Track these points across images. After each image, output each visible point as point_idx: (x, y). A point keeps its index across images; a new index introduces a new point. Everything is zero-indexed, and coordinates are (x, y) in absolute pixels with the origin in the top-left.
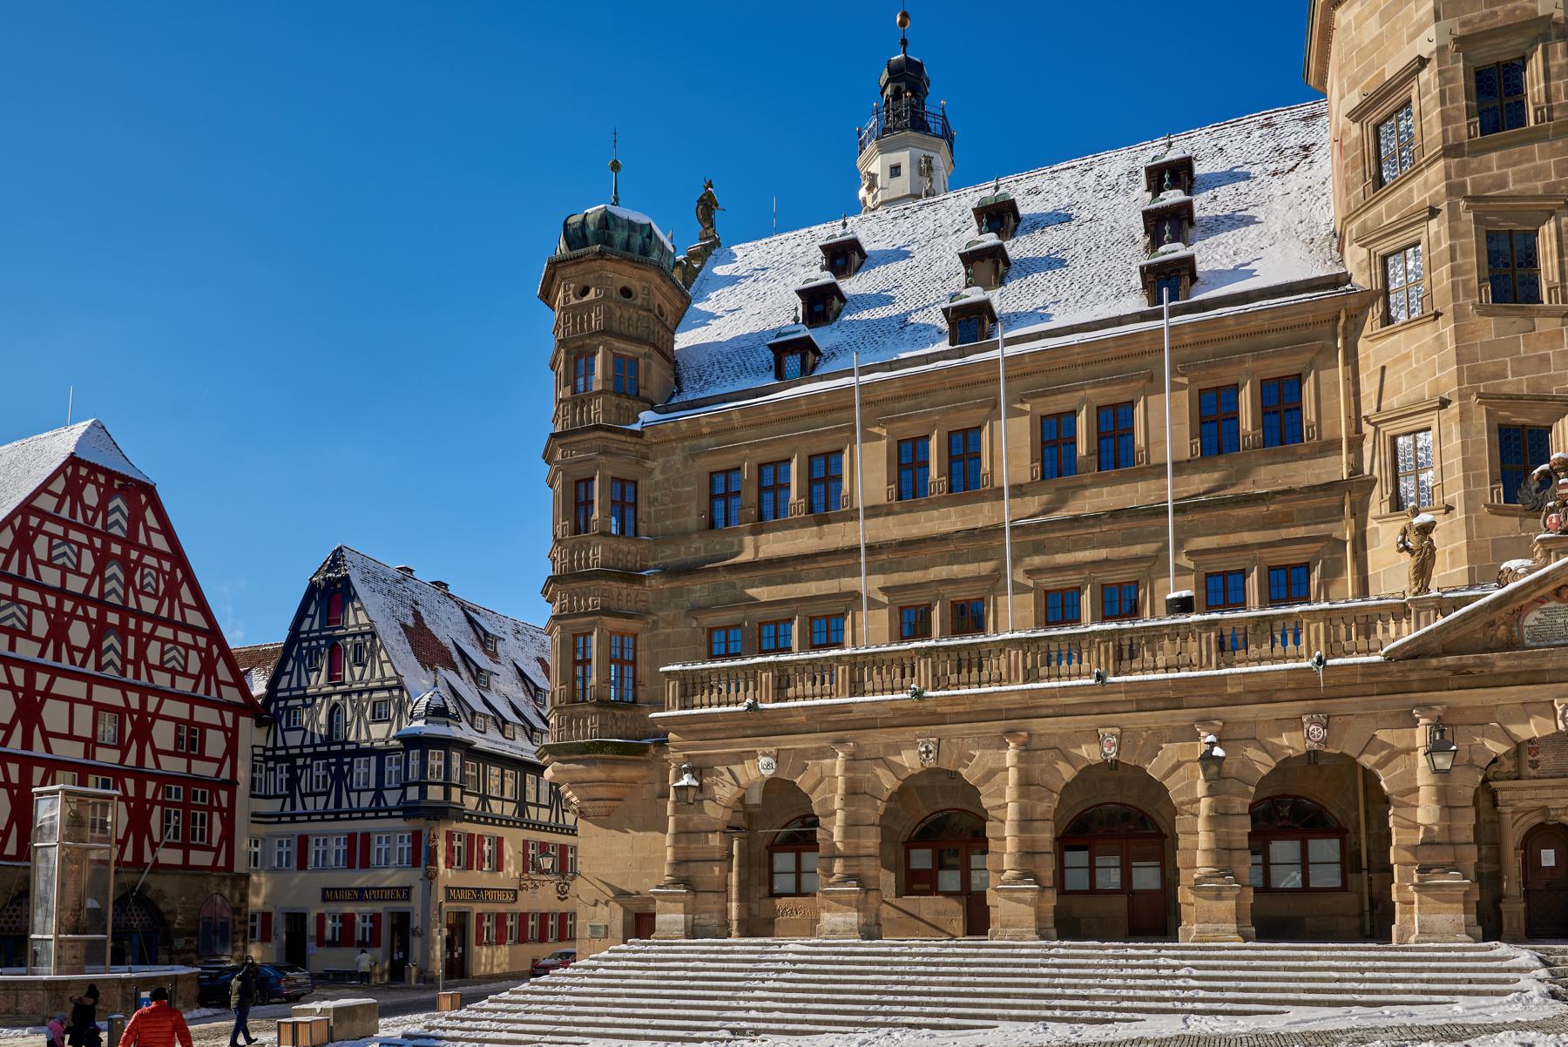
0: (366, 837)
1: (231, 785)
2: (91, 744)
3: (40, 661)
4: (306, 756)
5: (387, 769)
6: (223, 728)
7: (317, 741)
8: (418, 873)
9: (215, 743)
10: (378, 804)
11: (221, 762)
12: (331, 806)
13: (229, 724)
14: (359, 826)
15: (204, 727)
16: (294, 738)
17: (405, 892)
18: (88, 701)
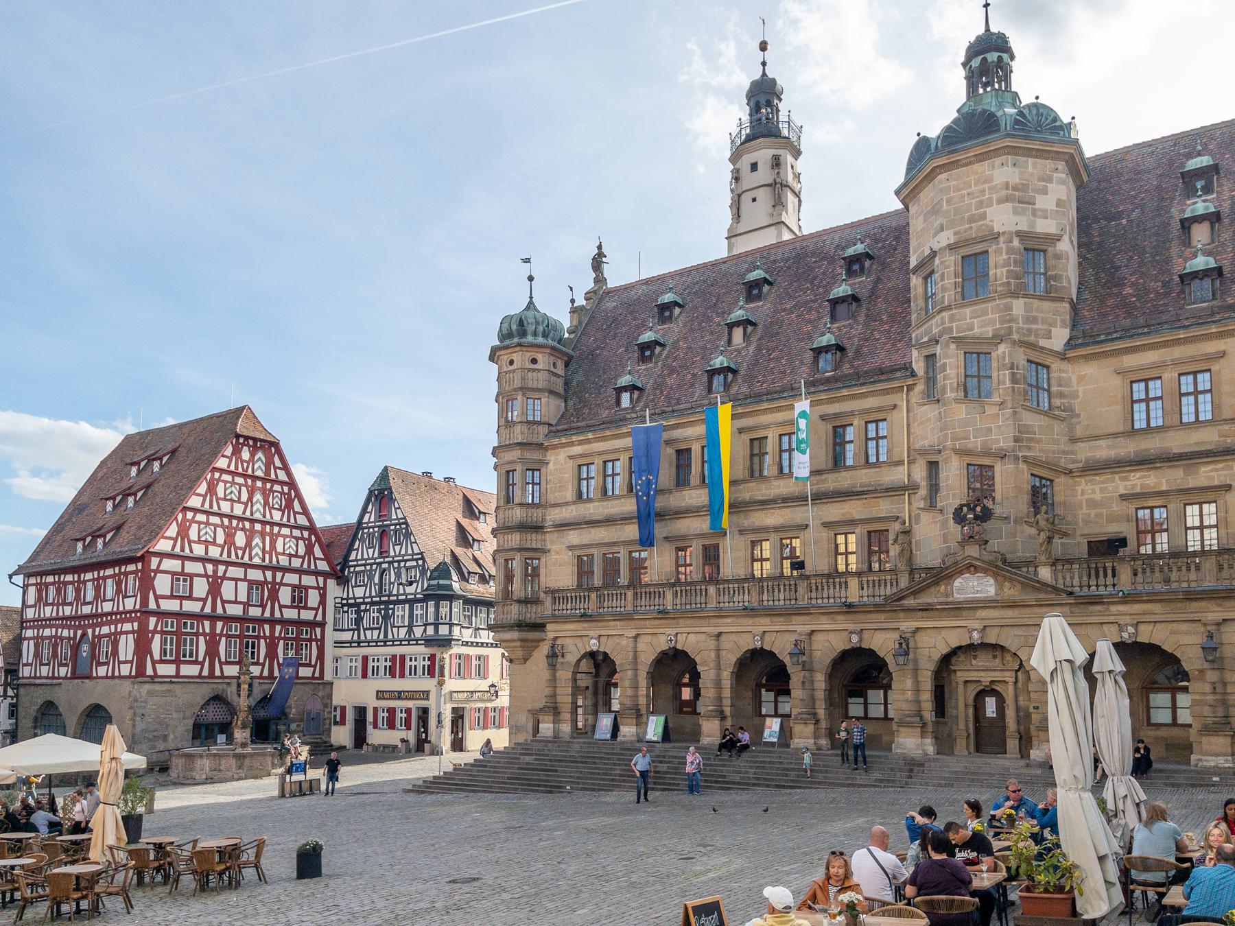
0: (403, 657)
1: (322, 625)
2: (247, 605)
3: (221, 559)
4: (366, 604)
5: (415, 612)
6: (318, 588)
7: (373, 594)
8: (435, 681)
9: (313, 598)
10: (410, 636)
11: (317, 610)
12: (382, 637)
13: (321, 585)
14: (398, 650)
15: (307, 588)
16: (359, 592)
17: (426, 695)
18: (245, 580)
